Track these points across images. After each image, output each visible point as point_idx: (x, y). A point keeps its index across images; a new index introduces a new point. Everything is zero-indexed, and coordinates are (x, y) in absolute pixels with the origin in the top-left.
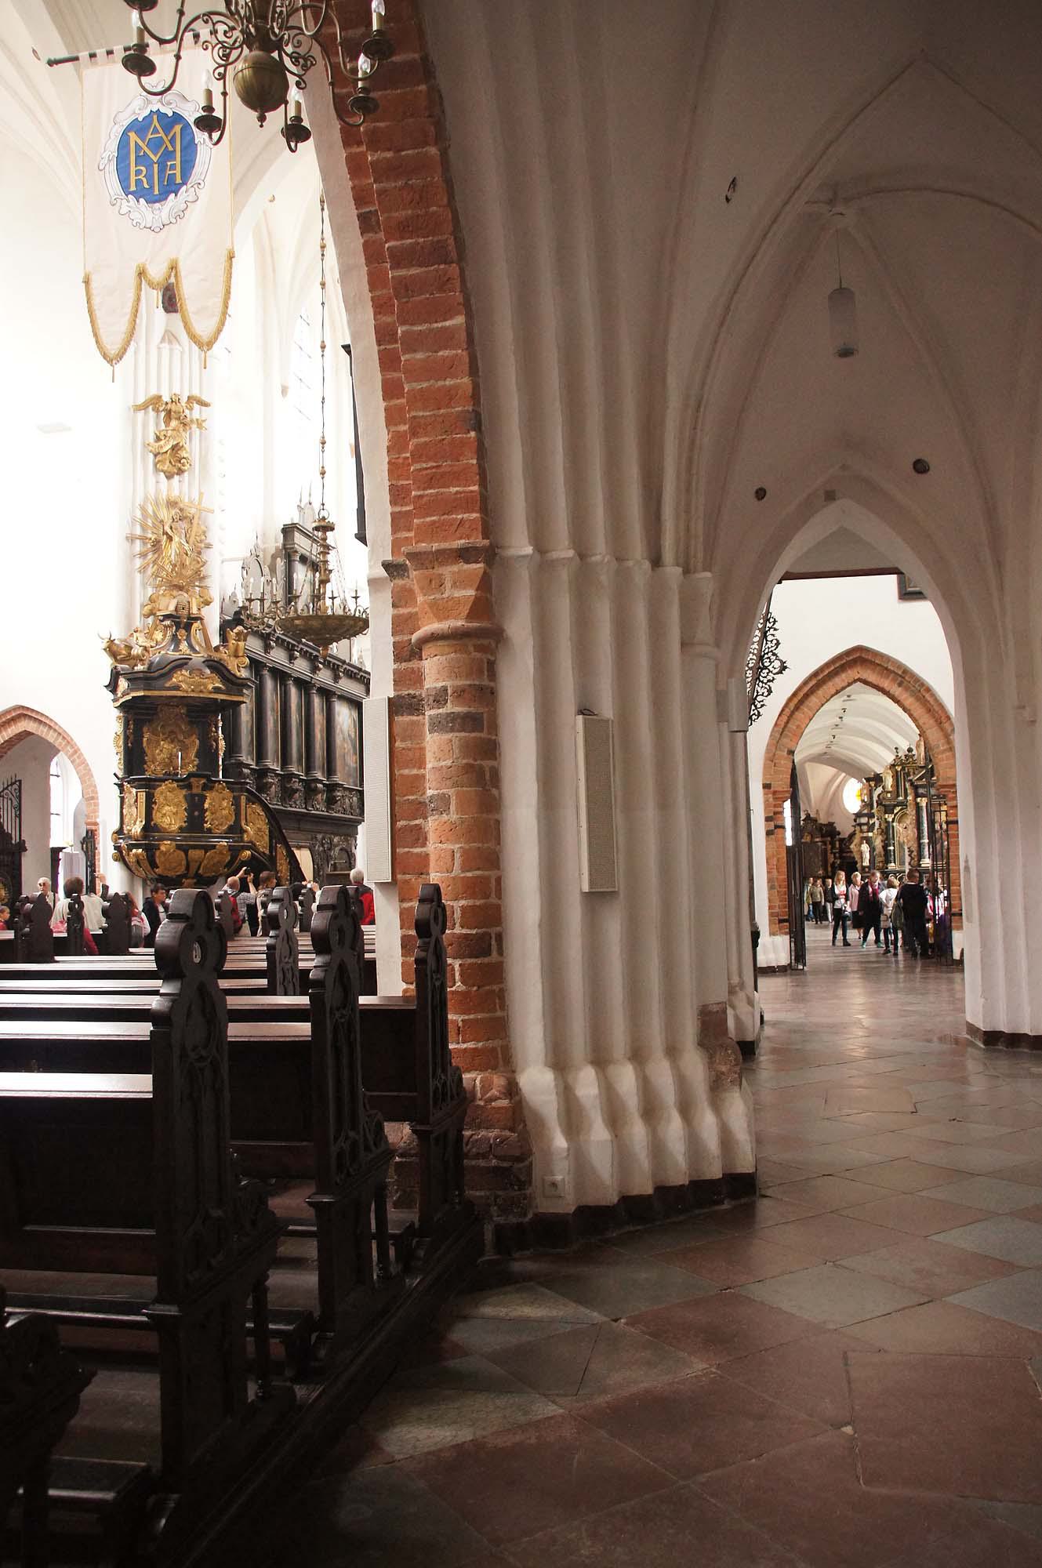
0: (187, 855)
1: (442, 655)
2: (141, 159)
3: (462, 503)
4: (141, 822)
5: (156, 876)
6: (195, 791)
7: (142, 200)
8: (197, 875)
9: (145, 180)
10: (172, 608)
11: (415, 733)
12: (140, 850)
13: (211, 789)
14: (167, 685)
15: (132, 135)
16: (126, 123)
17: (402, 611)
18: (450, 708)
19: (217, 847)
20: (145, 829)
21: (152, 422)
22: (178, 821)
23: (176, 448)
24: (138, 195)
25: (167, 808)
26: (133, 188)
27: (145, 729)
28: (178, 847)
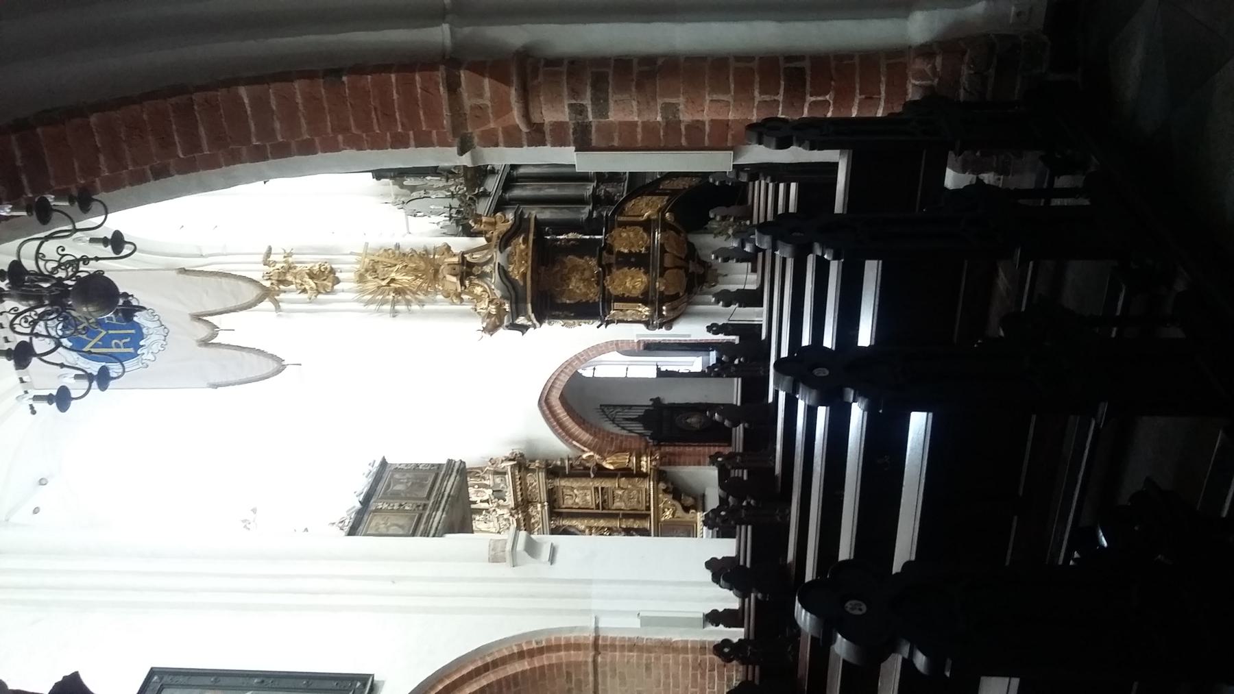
0: (668, 269)
1: (541, 108)
2: (106, 342)
3: (407, 88)
5: (686, 294)
6: (613, 259)
7: (142, 343)
8: (687, 259)
9: (124, 341)
10: (454, 279)
11: (606, 130)
12: (664, 308)
14: (521, 283)
17: (501, 139)
18: (587, 102)
20: (646, 304)
21: (289, 296)
23: (312, 275)
25: (628, 284)
26: (131, 350)
27: (559, 301)
28: (662, 275)
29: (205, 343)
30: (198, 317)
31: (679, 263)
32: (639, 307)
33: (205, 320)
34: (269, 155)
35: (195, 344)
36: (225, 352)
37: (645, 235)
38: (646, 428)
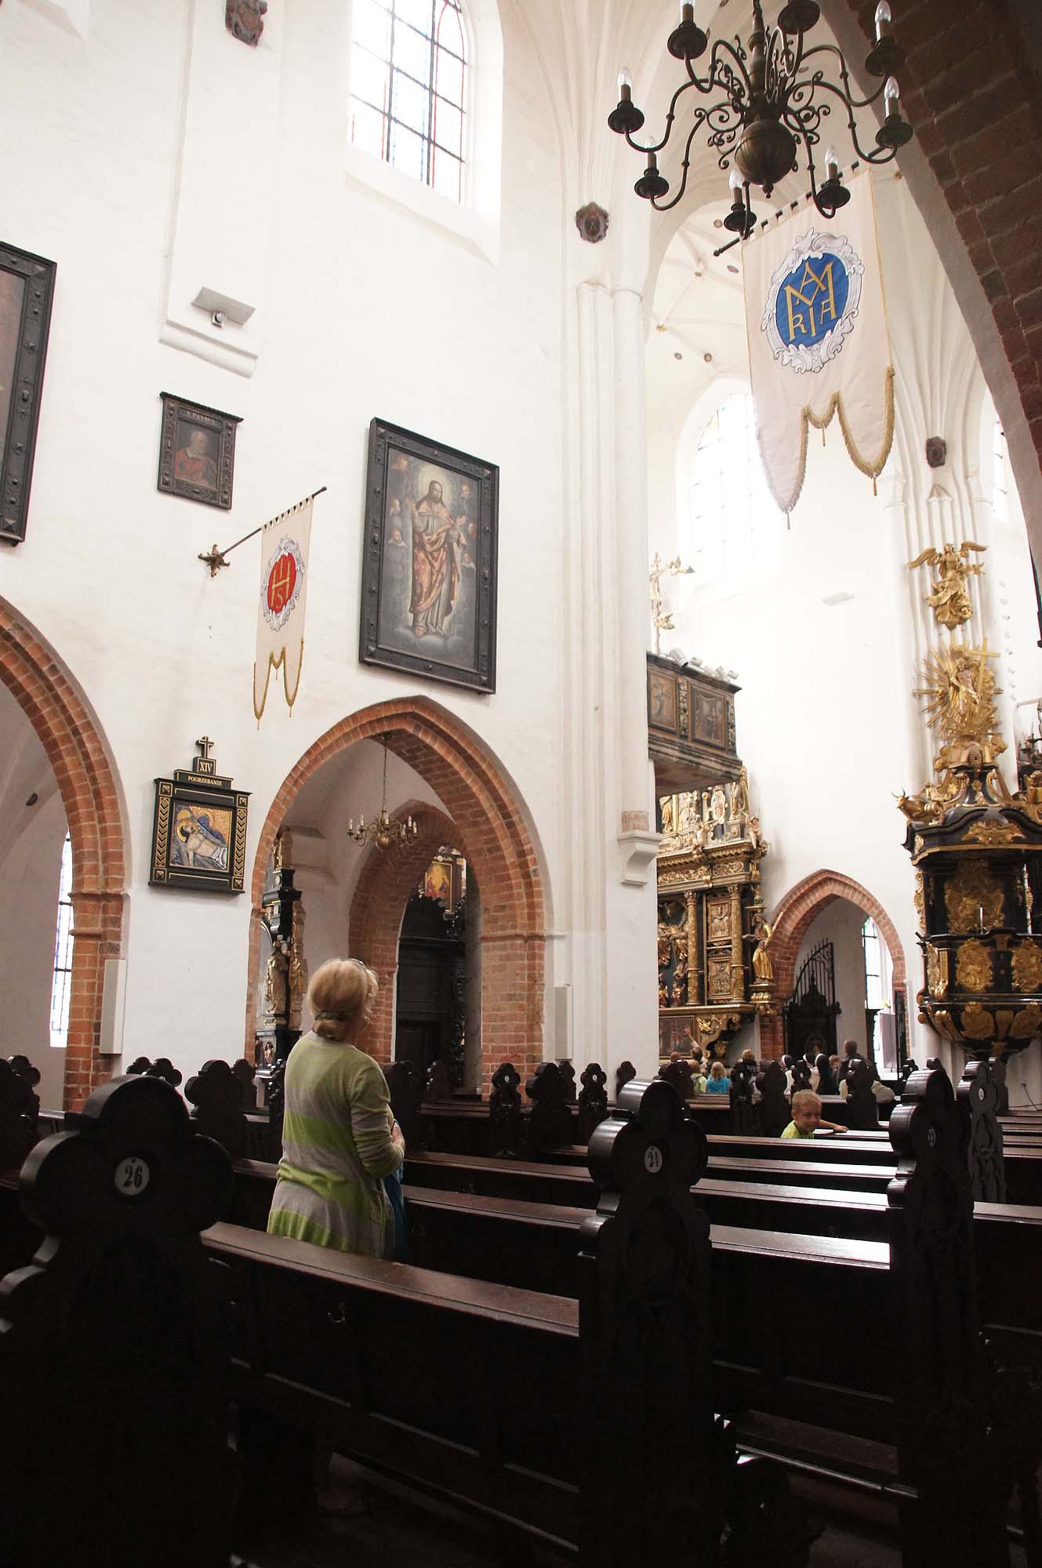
0: (994, 1017)
2: (798, 307)
4: (944, 982)
5: (963, 1039)
6: (1002, 947)
7: (801, 346)
8: (1007, 1038)
9: (802, 326)
12: (944, 1012)
13: (1018, 945)
15: (789, 290)
16: (781, 280)
19: (1027, 1007)
20: (948, 989)
22: (983, 981)
24: (796, 343)
25: (970, 967)
26: (792, 337)
27: (946, 886)
28: (985, 1008)
29: (807, 416)
30: (836, 402)
31: (1003, 1029)
32: (944, 982)
33: (833, 412)
34: (1034, 420)
35: (805, 405)
36: (798, 441)
37: (1035, 986)
38: (804, 997)
